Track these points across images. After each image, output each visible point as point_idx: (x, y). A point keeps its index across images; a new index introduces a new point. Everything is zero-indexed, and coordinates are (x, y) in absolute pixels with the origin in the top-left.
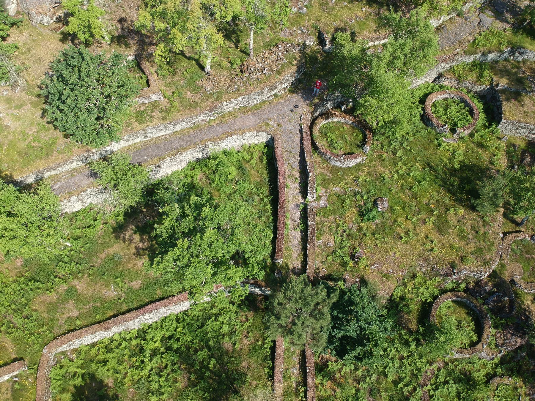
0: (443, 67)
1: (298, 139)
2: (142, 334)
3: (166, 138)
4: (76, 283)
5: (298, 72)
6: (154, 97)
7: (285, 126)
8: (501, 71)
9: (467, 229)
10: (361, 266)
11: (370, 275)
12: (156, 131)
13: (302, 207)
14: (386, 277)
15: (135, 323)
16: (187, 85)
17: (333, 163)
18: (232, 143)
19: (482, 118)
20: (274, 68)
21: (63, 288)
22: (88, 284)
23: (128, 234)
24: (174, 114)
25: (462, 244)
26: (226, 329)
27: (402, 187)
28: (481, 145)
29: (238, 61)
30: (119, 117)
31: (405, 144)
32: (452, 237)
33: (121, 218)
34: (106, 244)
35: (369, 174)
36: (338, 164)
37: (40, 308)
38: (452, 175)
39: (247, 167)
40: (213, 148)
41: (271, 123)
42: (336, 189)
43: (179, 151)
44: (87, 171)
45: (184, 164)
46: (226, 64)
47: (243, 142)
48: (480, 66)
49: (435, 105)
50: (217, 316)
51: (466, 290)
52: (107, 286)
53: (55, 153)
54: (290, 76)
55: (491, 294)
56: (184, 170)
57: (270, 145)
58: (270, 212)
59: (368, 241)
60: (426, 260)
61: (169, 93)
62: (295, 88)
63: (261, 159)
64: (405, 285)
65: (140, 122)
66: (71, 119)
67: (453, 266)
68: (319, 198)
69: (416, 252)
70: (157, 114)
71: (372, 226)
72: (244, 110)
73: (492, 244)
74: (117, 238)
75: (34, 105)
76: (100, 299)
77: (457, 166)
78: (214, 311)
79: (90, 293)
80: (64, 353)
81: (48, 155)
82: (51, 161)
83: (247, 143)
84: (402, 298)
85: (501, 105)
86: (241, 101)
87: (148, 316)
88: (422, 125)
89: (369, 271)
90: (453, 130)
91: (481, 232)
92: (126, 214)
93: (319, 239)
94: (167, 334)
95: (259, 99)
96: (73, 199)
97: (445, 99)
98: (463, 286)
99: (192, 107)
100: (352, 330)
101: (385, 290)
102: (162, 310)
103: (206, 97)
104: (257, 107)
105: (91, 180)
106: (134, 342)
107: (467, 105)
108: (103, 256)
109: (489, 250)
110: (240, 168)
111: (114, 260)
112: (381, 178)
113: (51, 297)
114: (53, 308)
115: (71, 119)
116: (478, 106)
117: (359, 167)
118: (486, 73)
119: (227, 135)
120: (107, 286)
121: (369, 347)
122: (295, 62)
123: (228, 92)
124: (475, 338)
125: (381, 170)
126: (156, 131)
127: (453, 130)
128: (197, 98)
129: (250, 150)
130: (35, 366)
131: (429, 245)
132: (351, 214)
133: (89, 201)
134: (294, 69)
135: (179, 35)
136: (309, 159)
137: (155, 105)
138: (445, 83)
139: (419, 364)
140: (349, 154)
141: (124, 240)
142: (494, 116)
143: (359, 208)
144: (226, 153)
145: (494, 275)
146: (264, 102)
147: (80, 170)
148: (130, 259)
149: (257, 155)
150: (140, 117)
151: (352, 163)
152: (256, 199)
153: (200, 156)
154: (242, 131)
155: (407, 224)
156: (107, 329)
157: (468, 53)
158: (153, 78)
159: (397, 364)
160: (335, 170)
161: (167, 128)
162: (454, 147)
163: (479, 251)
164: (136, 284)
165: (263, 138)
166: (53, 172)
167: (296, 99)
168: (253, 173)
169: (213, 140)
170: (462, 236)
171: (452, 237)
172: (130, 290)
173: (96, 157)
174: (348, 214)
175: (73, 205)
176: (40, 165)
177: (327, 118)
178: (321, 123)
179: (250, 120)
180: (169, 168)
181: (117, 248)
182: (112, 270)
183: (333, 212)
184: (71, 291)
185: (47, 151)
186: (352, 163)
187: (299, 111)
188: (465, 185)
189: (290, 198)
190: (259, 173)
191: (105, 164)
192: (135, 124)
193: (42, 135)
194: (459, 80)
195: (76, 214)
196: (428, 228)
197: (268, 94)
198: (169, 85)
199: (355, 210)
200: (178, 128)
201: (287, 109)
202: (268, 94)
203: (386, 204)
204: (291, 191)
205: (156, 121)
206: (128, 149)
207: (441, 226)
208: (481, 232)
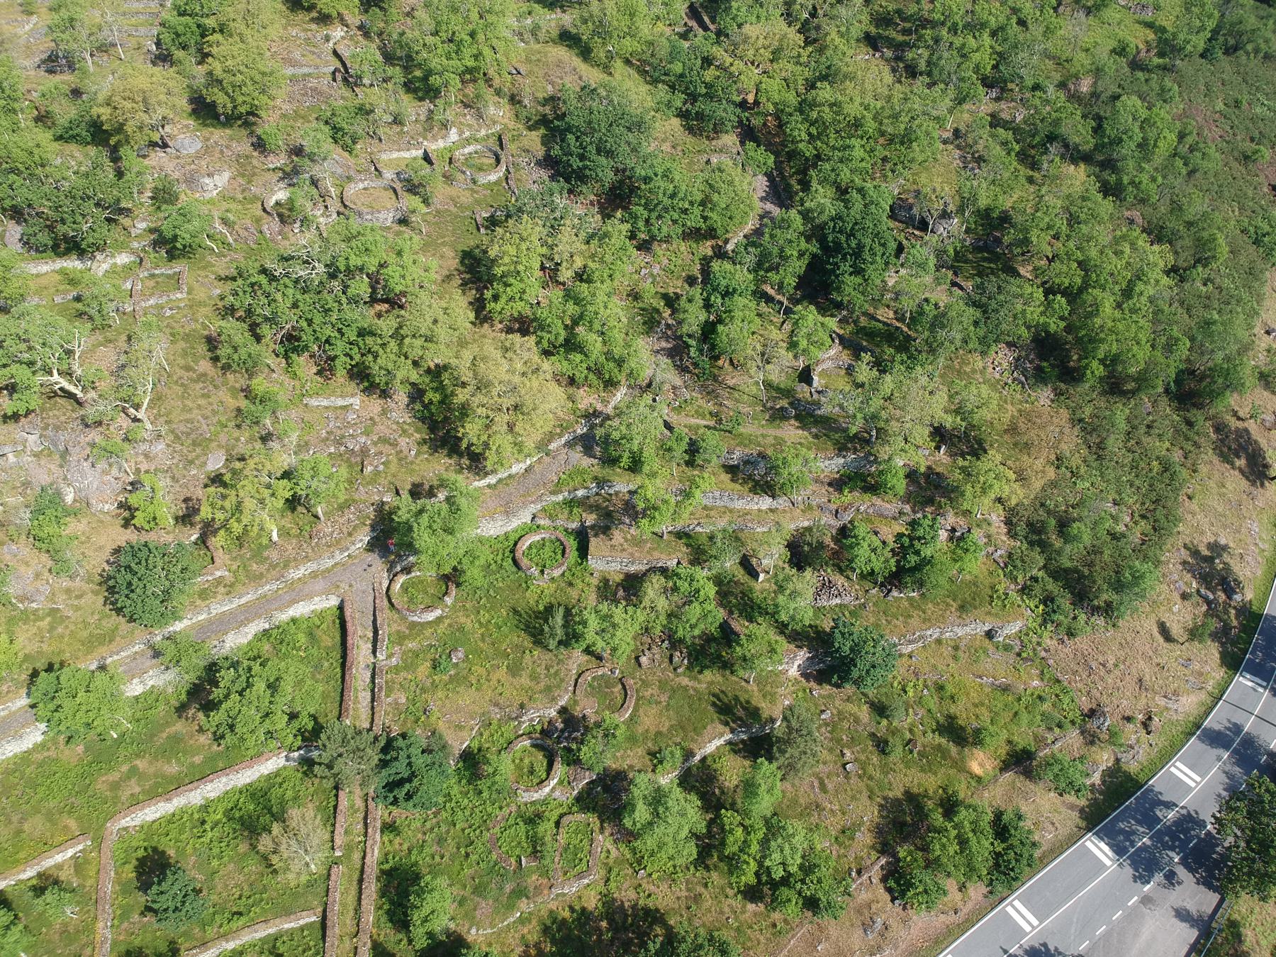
0: (534, 508)
1: (371, 599)
2: (205, 808)
3: (231, 612)
4: (138, 762)
5: (373, 528)
6: (218, 574)
7: (356, 586)
8: (591, 506)
9: (541, 670)
10: (433, 719)
11: (442, 726)
12: (220, 607)
13: (371, 666)
14: (460, 727)
15: (195, 797)
16: (253, 557)
17: (411, 619)
18: (300, 610)
19: (573, 555)
20: (345, 530)
21: (125, 768)
22: (151, 763)
23: (191, 712)
24: (239, 587)
25: (532, 684)
26: (289, 794)
27: (482, 635)
28: (571, 584)
29: (308, 528)
30: (184, 599)
31: (491, 592)
32: (525, 680)
33: (184, 697)
34: (167, 724)
35: (450, 625)
36: (415, 619)
37: (104, 787)
38: (537, 617)
39: (319, 633)
40: (284, 617)
41: (342, 585)
42: (411, 645)
43: (243, 624)
44: (150, 653)
45: (250, 637)
46: (295, 531)
47: (313, 607)
48: (571, 503)
49: (530, 548)
50: (281, 784)
51: (543, 731)
52: (169, 762)
53: (118, 639)
54: (364, 537)
55: (562, 731)
56: (249, 643)
57: (341, 608)
58: (339, 675)
59: (440, 694)
60: (496, 705)
61: (234, 567)
62: (372, 546)
63: (334, 622)
64: (481, 735)
65: (204, 600)
66: (139, 605)
67: (522, 706)
68: (390, 656)
69: (487, 698)
70: (221, 589)
71: (446, 678)
72: (314, 575)
73: (562, 680)
74: (180, 717)
75: (96, 593)
76: (164, 777)
77: (541, 608)
78: (279, 780)
79: (152, 770)
80: (126, 829)
81: (110, 641)
82: (113, 647)
83: (319, 607)
84: (480, 750)
85: (588, 542)
86: (311, 566)
87: (209, 787)
88: (514, 569)
89: (440, 723)
90: (542, 572)
91: (552, 671)
92: (189, 693)
93: (387, 696)
94: (230, 805)
95: (330, 563)
96: (135, 681)
97: (543, 539)
98: (538, 728)
99: (257, 578)
100: (400, 768)
101: (459, 742)
102: (224, 779)
103: (273, 566)
104: (328, 570)
105: (154, 661)
106: (196, 816)
107: (562, 544)
108: (164, 735)
109: (558, 687)
110: (311, 635)
111: (176, 739)
112: (461, 629)
113: (114, 776)
114: (115, 786)
115: (139, 605)
116: (572, 544)
117: (439, 620)
118: (575, 510)
119: (294, 602)
120: (169, 762)
121: (416, 782)
122: (368, 522)
123: (295, 559)
124: (544, 776)
125: (463, 620)
126: (220, 607)
127: (542, 572)
128: (263, 568)
129: (321, 615)
130: (99, 841)
131: (500, 689)
132: (424, 668)
133: (151, 683)
134: (368, 529)
135: (236, 525)
136: (385, 615)
137: (219, 581)
138: (542, 522)
139: (489, 809)
140: (428, 608)
141: (187, 719)
142: (583, 551)
143: (434, 660)
144: (294, 620)
145: (563, 711)
146: (336, 564)
147: (142, 654)
148: (192, 736)
149: (330, 619)
150: (204, 594)
151: (430, 616)
152: (326, 664)
153: (267, 626)
154: (309, 597)
155: (482, 671)
156: (169, 800)
157: (553, 493)
158: (220, 556)
159: (467, 813)
160: (413, 625)
161: (231, 602)
162: (542, 587)
163: (548, 689)
164: (198, 759)
165: (334, 601)
166: (116, 657)
167: (374, 558)
168: (324, 637)
169: (281, 609)
170: (534, 677)
171: (525, 680)
172: (192, 765)
173: (159, 638)
174: (421, 669)
175: (135, 688)
176: (103, 650)
177: (409, 572)
178: (402, 579)
179: (320, 584)
180: (236, 641)
181: (179, 727)
182: (175, 746)
183: (406, 668)
184: (134, 771)
185: (108, 638)
186: (430, 616)
187: (373, 569)
188: (535, 625)
189: (361, 659)
190: (330, 638)
191: (168, 642)
192: (198, 602)
193: (104, 623)
194: (551, 517)
195: (137, 698)
196: (502, 674)
197: (339, 557)
198: (234, 559)
199: (428, 664)
200: (243, 601)
201: (360, 569)
202: (339, 557)
203: (460, 655)
204: (361, 653)
205: (220, 597)
206: (191, 627)
207: (514, 670)
208: (552, 671)
